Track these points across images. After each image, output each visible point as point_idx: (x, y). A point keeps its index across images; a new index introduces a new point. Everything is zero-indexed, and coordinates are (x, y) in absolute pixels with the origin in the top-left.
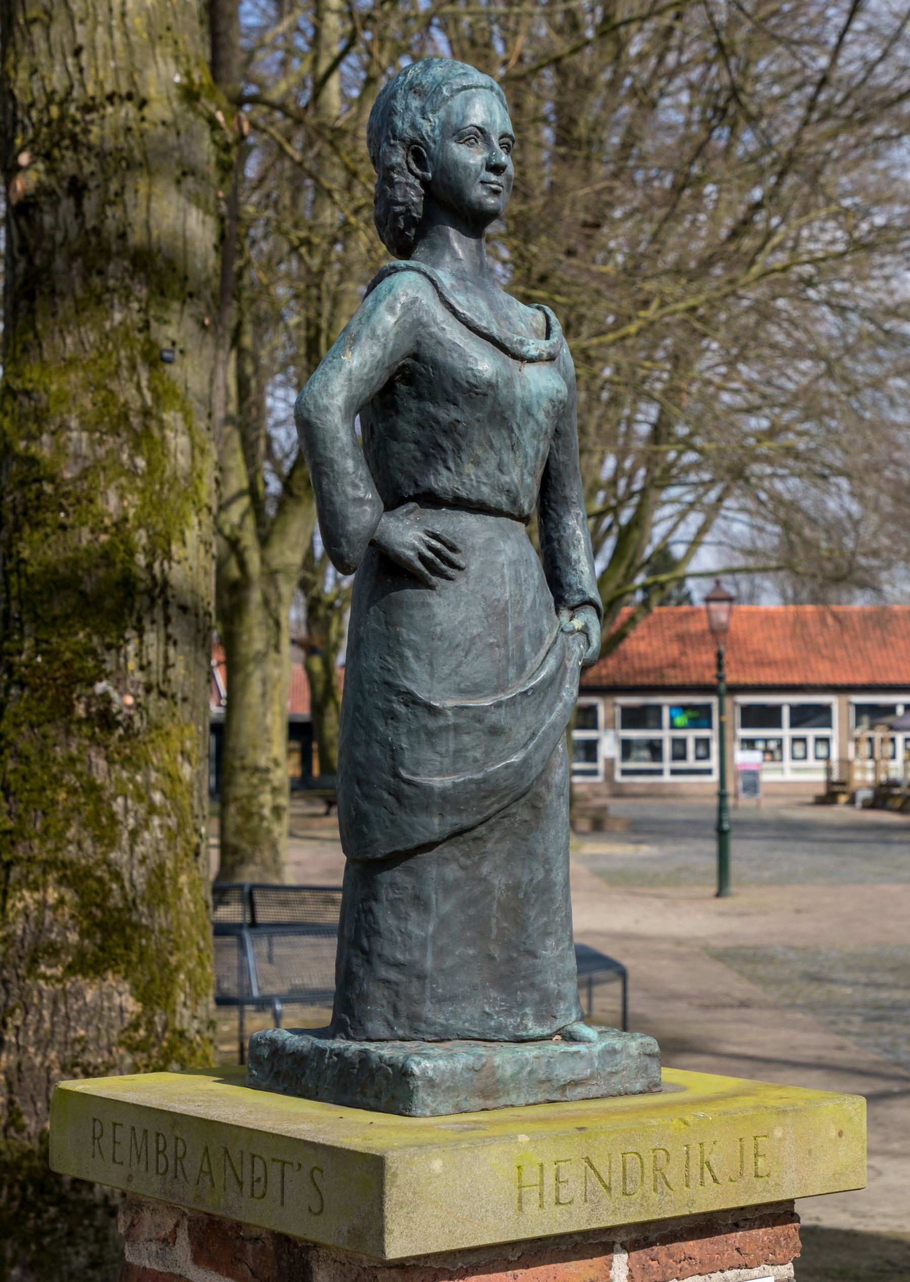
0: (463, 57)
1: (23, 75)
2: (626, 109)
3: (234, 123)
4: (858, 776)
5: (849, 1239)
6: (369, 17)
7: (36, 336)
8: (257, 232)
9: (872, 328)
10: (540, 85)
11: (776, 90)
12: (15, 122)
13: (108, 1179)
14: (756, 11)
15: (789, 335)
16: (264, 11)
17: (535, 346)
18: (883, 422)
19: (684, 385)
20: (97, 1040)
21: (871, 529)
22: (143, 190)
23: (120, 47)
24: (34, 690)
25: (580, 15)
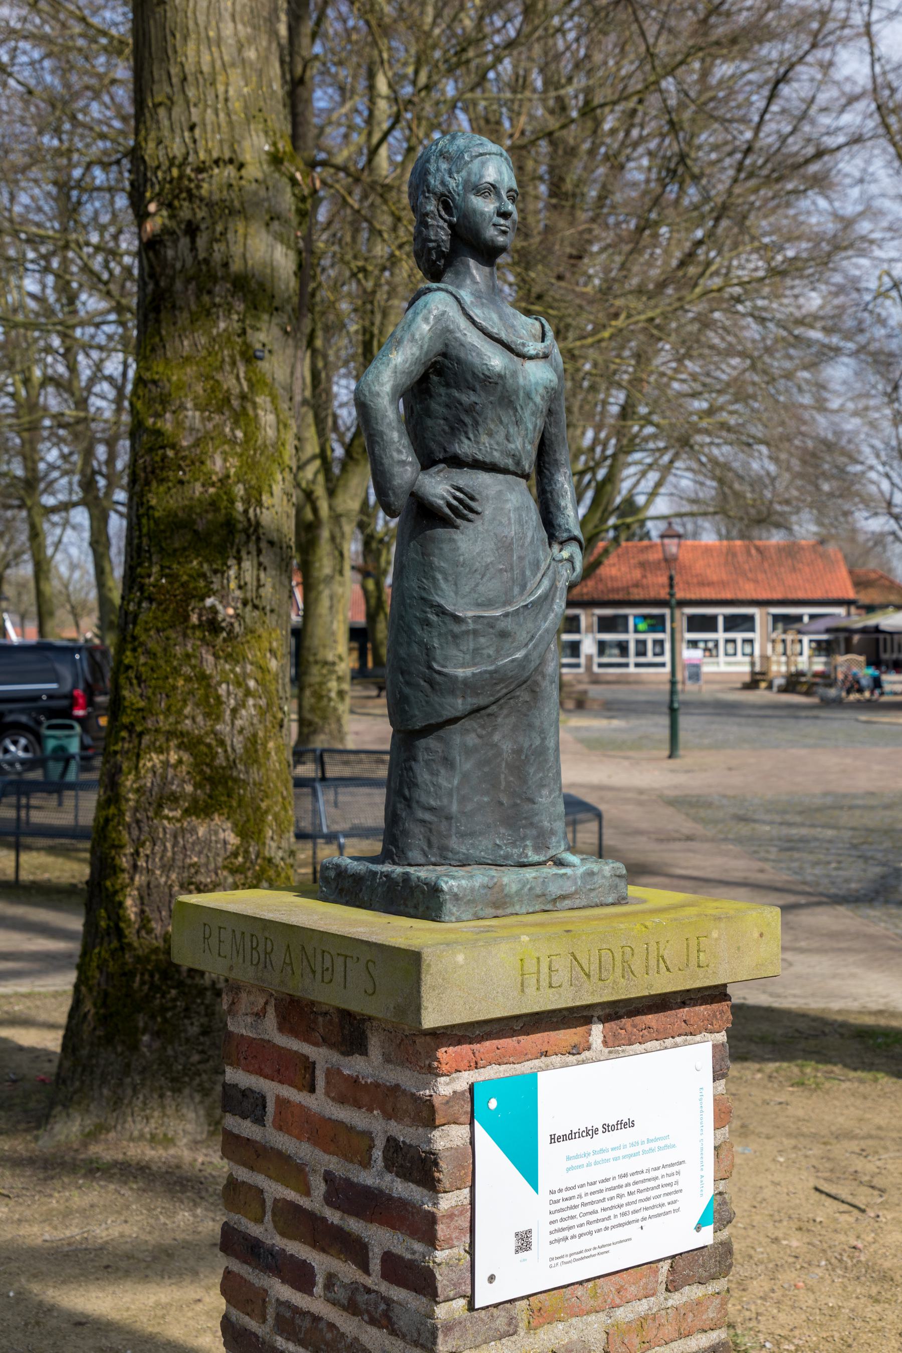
0: (480, 132)
1: (151, 145)
2: (601, 171)
3: (309, 180)
4: (774, 668)
5: (768, 1014)
6: (410, 102)
7: (161, 340)
8: (326, 262)
9: (785, 334)
10: (537, 153)
11: (714, 156)
12: (146, 180)
13: (215, 968)
14: (698, 98)
15: (723, 339)
16: (331, 97)
17: (533, 347)
18: (793, 404)
19: (644, 376)
20: (207, 865)
21: (785, 484)
22: (241, 231)
23: (224, 124)
24: (160, 604)
25: (567, 100)
